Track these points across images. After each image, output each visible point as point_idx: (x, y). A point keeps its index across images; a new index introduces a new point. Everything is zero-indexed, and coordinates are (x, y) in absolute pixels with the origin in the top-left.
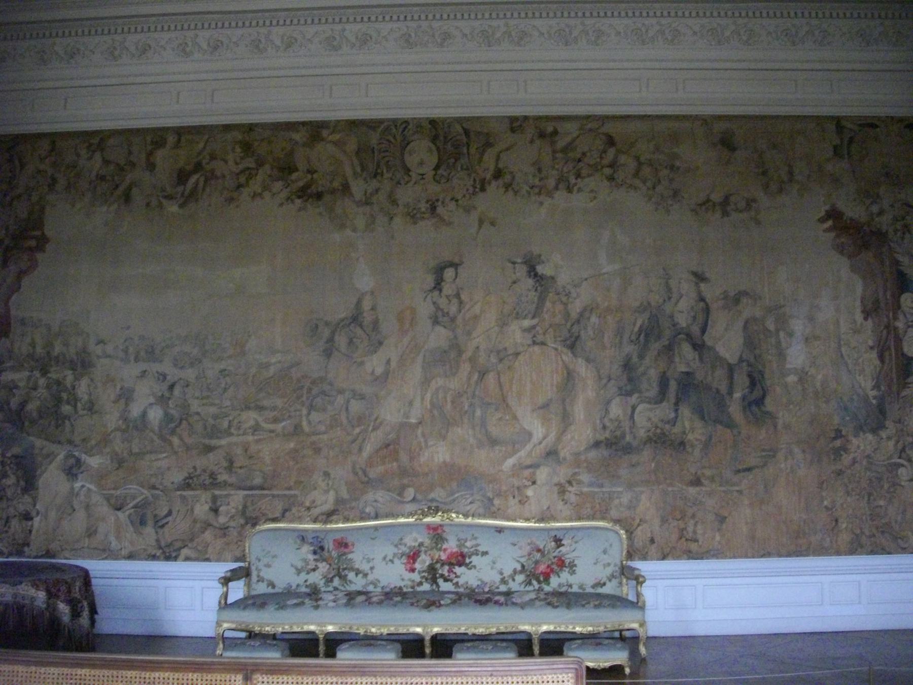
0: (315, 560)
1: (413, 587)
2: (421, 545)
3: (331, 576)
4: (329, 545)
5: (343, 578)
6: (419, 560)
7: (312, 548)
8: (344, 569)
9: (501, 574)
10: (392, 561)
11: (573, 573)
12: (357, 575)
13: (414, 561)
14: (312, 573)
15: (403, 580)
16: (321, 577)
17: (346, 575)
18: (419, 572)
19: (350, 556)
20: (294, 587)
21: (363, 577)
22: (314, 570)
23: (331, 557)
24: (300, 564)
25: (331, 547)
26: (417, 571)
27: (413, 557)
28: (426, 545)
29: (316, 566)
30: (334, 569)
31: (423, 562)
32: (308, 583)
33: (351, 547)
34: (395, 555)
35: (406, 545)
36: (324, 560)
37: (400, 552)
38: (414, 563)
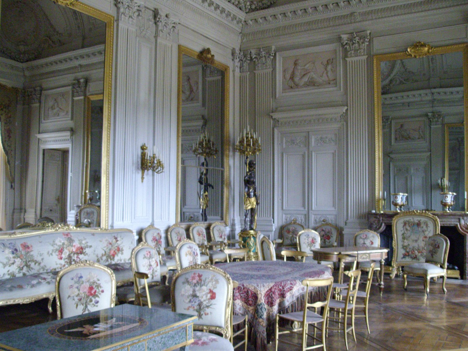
0: (14, 257)
2: (63, 244)
3: (22, 266)
4: (20, 248)
5: (28, 266)
6: (64, 252)
8: (29, 261)
10: (52, 254)
12: (35, 264)
13: (62, 253)
14: (12, 266)
15: (57, 264)
16: (17, 268)
17: (30, 265)
18: (64, 259)
19: (32, 253)
21: (38, 265)
22: (13, 264)
23: (22, 255)
24: (5, 261)
25: (21, 249)
26: (63, 259)
27: (61, 251)
28: (66, 244)
29: (14, 261)
30: (24, 262)
31: (65, 255)
33: (31, 248)
34: (53, 250)
35: (57, 245)
36: (19, 257)
37: (55, 248)
38: (62, 254)
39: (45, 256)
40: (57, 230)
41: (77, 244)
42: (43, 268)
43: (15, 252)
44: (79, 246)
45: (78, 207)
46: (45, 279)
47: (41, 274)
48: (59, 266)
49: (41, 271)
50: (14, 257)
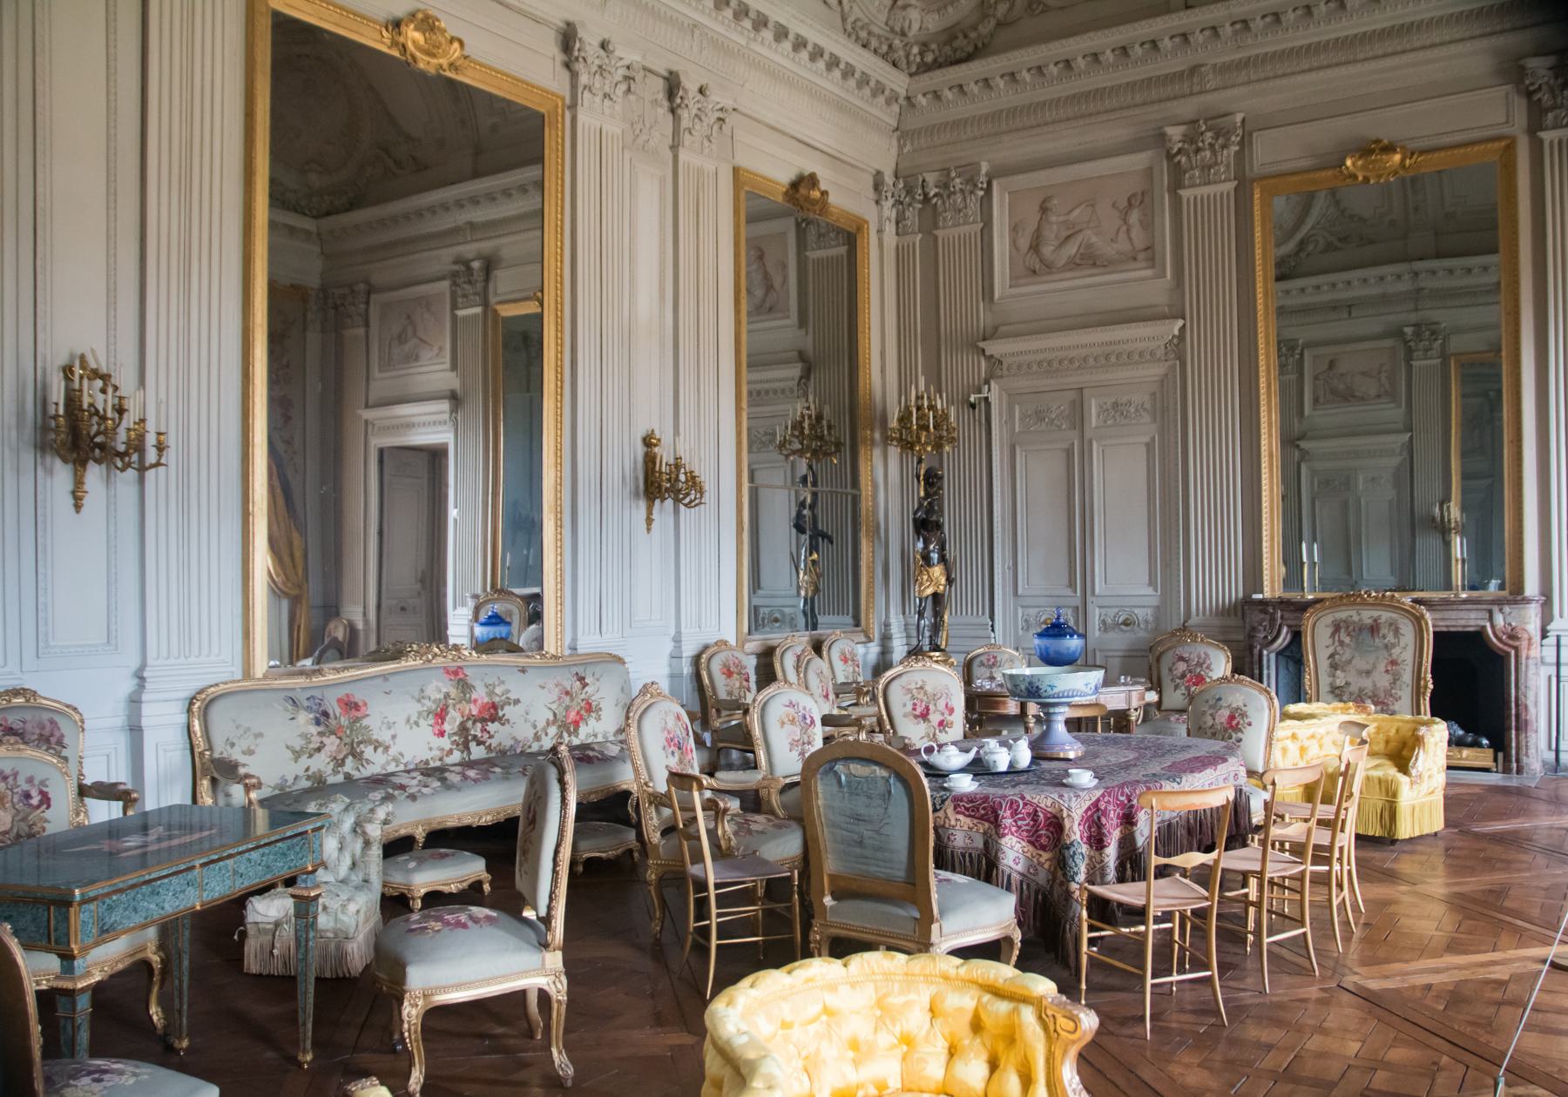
0: (321, 734)
1: (441, 759)
2: (447, 696)
3: (341, 756)
4: (334, 708)
5: (357, 756)
7: (312, 716)
9: (535, 727)
10: (417, 724)
11: (598, 719)
12: (375, 749)
14: (317, 755)
18: (450, 736)
19: (365, 722)
20: (290, 780)
22: (319, 750)
23: (341, 727)
24: (298, 743)
25: (338, 711)
27: (441, 715)
28: (453, 696)
32: (310, 773)
33: (363, 709)
34: (420, 713)
36: (333, 733)
39: (402, 729)
40: (430, 661)
41: (480, 694)
42: (394, 759)
43: (322, 719)
44: (486, 700)
45: (475, 597)
46: (402, 787)
47: (392, 774)
48: (437, 753)
49: (391, 768)
50: (321, 734)
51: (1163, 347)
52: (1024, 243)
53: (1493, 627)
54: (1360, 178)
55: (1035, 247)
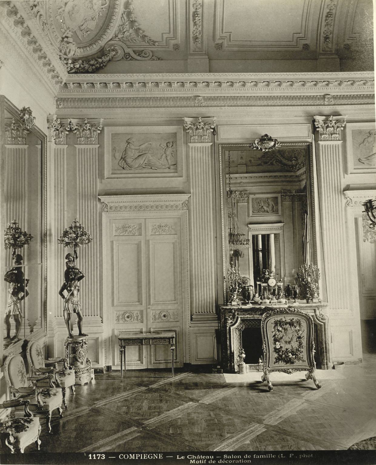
51: (181, 205)
52: (118, 155)
53: (316, 315)
54: (259, 149)
55: (123, 159)
